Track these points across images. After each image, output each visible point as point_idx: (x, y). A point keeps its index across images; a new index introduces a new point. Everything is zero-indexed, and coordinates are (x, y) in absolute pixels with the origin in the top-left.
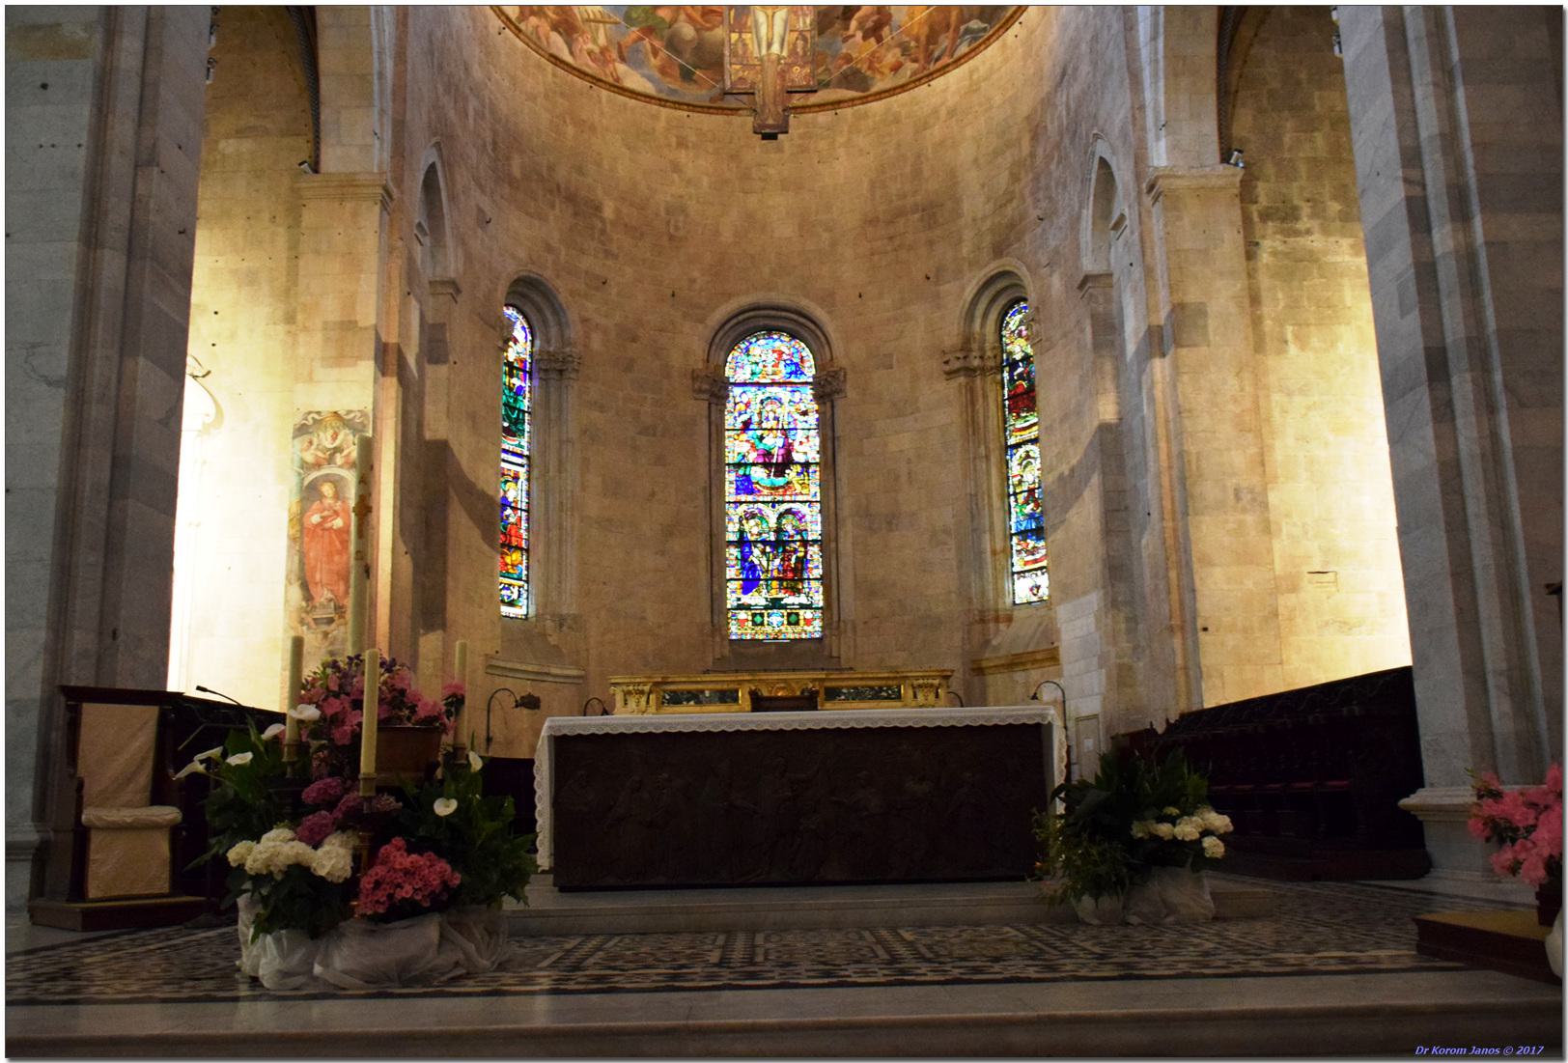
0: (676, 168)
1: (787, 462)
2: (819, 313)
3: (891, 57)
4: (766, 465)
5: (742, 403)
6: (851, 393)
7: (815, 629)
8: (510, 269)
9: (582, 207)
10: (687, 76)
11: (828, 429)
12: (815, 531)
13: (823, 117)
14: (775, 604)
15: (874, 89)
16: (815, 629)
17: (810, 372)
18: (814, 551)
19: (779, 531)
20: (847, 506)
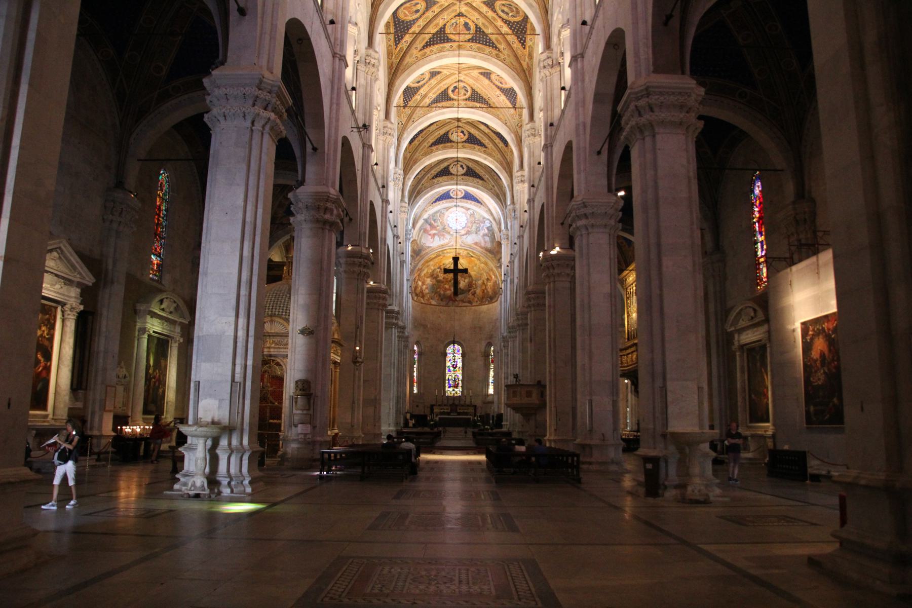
0: (440, 317)
1: (456, 367)
2: (462, 342)
3: (476, 299)
4: (453, 367)
5: (450, 357)
6: (467, 357)
7: (459, 394)
8: (416, 340)
9: (425, 326)
10: (442, 300)
11: (463, 361)
12: (461, 378)
13: (465, 308)
14: (454, 390)
15: (473, 304)
16: (459, 394)
17: (461, 352)
18: (460, 382)
19: (455, 378)
20: (465, 376)
